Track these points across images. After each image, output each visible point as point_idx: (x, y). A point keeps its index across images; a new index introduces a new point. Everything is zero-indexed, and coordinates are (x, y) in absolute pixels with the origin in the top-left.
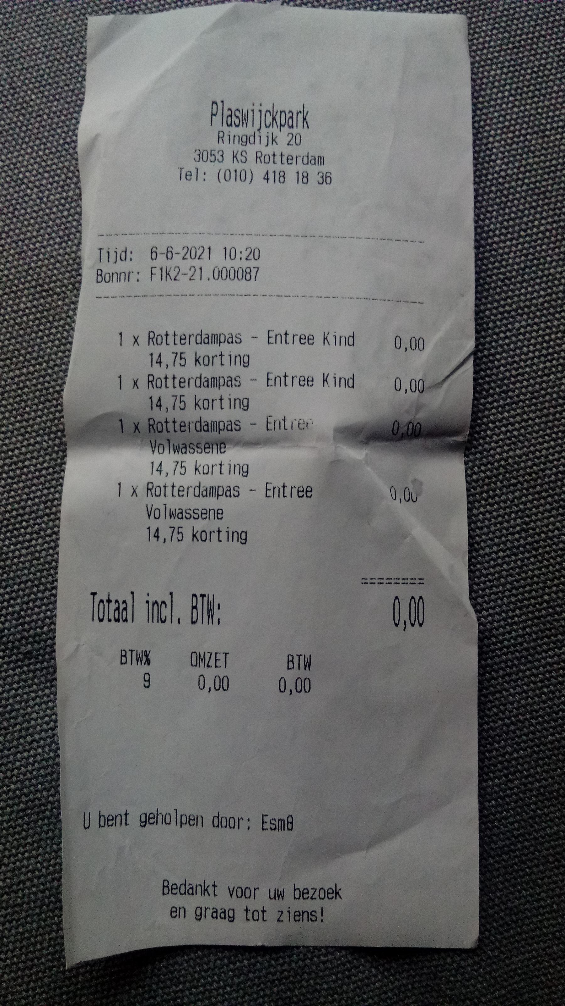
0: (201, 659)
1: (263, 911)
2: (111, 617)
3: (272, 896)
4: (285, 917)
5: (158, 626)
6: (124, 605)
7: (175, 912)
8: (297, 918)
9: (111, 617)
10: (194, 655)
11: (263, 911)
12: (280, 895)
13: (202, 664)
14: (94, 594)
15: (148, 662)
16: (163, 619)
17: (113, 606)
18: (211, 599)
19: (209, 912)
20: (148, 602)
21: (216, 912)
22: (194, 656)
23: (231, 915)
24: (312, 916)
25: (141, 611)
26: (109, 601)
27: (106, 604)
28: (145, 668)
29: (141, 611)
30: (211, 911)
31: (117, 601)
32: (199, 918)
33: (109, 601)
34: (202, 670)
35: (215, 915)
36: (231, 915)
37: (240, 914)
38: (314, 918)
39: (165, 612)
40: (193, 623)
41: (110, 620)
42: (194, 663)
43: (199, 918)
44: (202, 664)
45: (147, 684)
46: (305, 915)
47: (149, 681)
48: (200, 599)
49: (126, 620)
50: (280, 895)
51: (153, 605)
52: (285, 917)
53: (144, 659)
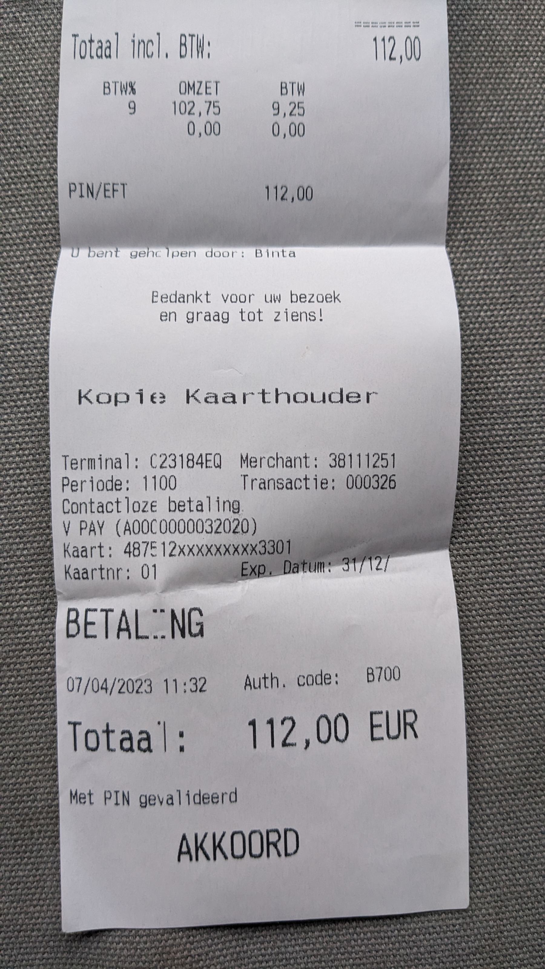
0: (190, 87)
1: (259, 312)
2: (94, 54)
3: (268, 299)
4: (282, 316)
5: (143, 61)
6: (108, 44)
7: (164, 317)
8: (295, 318)
9: (94, 54)
10: (183, 85)
11: (259, 312)
12: (276, 299)
13: (191, 92)
14: (75, 36)
15: (133, 90)
16: (150, 54)
17: (95, 45)
18: (200, 37)
19: (201, 317)
20: (133, 41)
21: (210, 316)
22: (183, 85)
23: (225, 316)
24: (310, 316)
25: (125, 47)
26: (91, 41)
27: (88, 44)
28: (131, 97)
29: (125, 47)
30: (204, 314)
31: (100, 41)
32: (190, 321)
33: (91, 41)
34: (191, 96)
35: (207, 318)
36: (225, 316)
37: (235, 317)
38: (312, 318)
39: (152, 49)
40: (181, 56)
41: (92, 57)
42: (183, 90)
43: (190, 321)
44: (191, 92)
45: (132, 111)
46: (304, 315)
47: (135, 108)
48: (189, 39)
49: (110, 56)
50: (276, 299)
51: (139, 43)
52: (282, 316)
53: (129, 89)
